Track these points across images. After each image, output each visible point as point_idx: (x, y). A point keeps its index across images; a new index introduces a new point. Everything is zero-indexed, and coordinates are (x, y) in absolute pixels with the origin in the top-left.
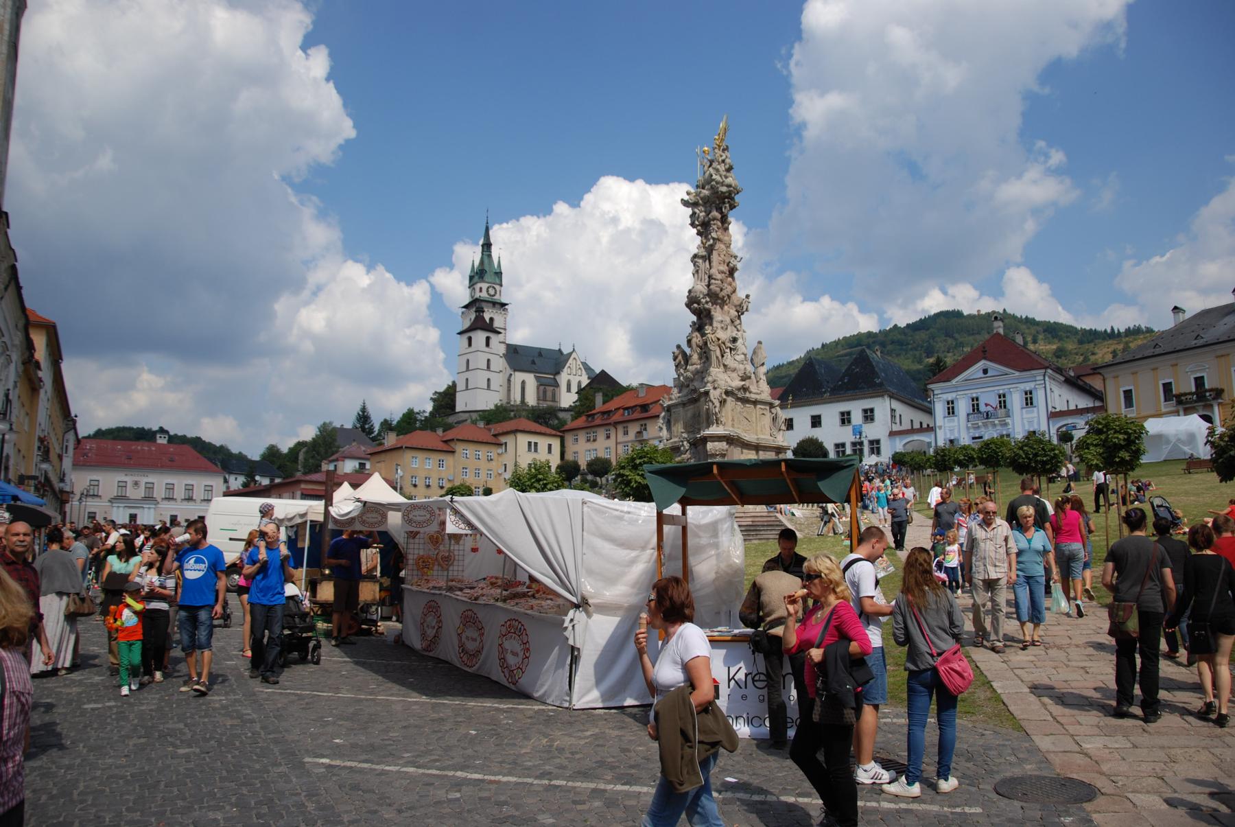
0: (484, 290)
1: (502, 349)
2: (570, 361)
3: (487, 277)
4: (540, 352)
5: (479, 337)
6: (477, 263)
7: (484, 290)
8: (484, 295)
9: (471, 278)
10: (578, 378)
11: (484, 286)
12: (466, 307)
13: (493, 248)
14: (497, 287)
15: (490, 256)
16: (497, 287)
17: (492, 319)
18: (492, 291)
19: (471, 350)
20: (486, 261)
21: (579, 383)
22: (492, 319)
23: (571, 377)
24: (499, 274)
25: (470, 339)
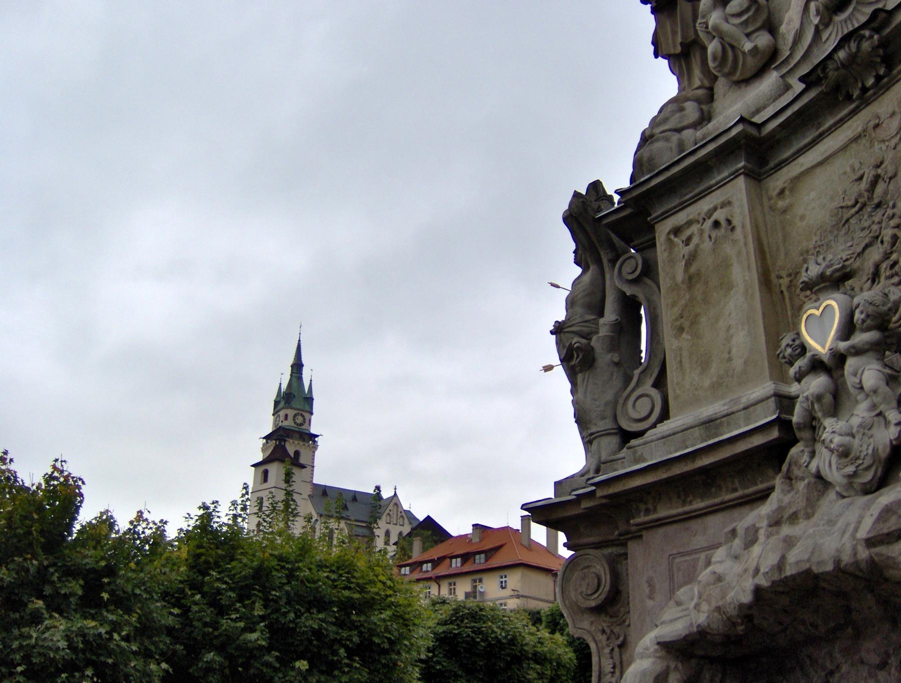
0: (290, 418)
1: (307, 490)
2: (391, 507)
3: (295, 403)
4: (356, 496)
5: (276, 471)
6: (284, 387)
7: (290, 418)
8: (289, 423)
9: (277, 403)
10: (398, 529)
11: (291, 413)
12: (266, 438)
13: (304, 368)
14: (306, 415)
15: (300, 378)
16: (306, 415)
17: (297, 453)
18: (299, 420)
19: (265, 486)
20: (295, 384)
21: (400, 534)
22: (297, 453)
23: (391, 527)
24: (309, 400)
25: (266, 473)
